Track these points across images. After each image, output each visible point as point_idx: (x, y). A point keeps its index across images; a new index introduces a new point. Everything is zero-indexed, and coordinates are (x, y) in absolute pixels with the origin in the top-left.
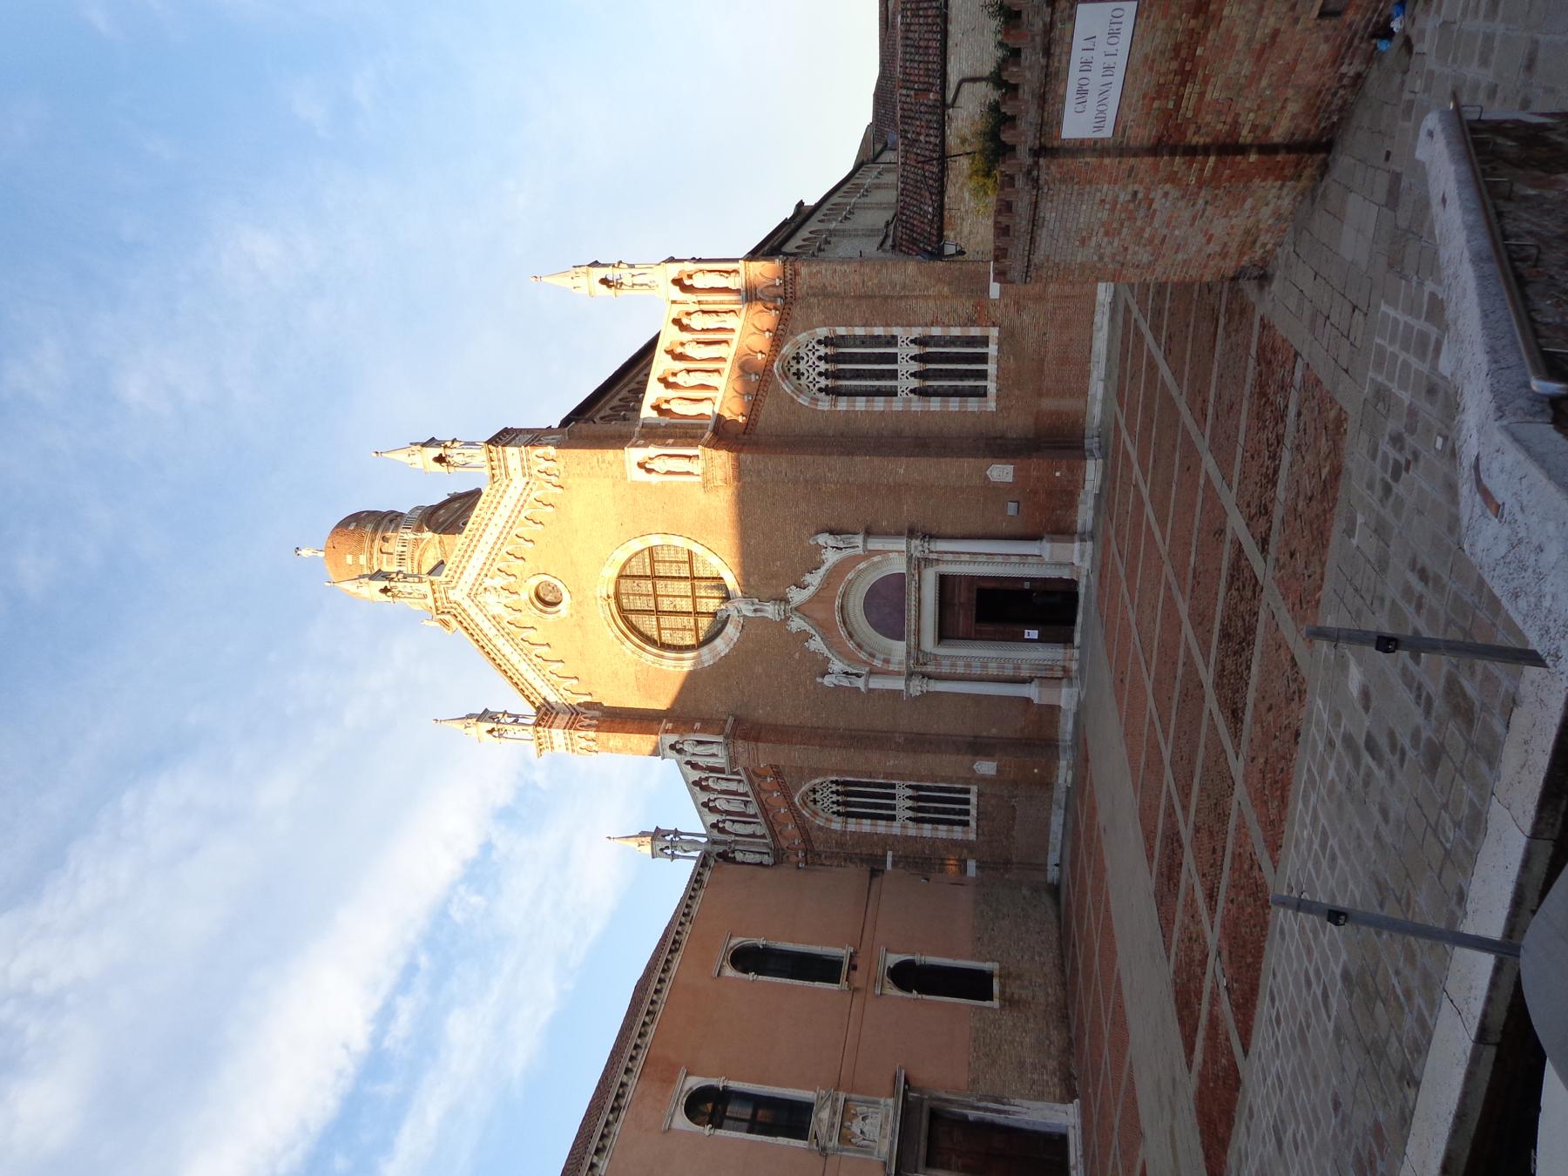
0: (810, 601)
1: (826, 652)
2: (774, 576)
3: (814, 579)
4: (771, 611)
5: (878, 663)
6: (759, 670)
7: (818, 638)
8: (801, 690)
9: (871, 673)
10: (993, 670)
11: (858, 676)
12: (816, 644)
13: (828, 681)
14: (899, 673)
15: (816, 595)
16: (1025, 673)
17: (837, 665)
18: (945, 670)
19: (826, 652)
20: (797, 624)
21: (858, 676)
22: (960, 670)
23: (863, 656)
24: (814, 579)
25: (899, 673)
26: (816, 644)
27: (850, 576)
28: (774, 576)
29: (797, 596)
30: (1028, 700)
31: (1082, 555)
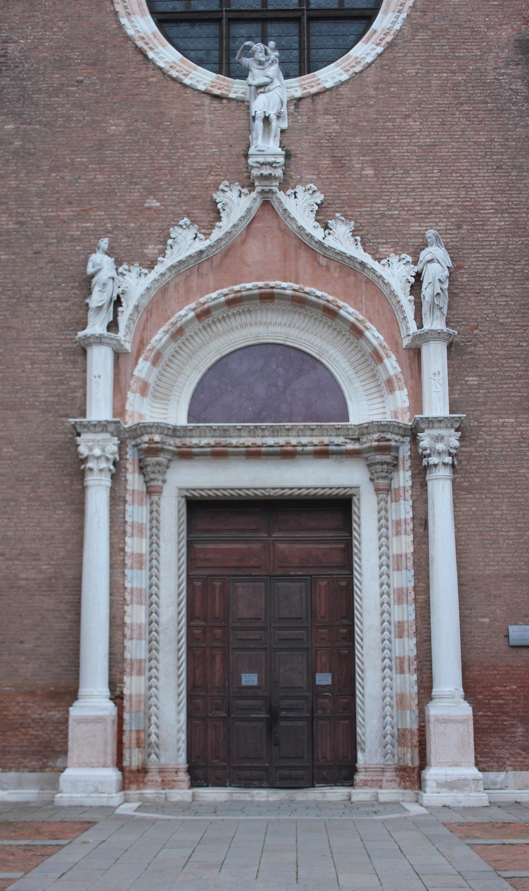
0: (285, 231)
1: (171, 258)
2: (339, 164)
3: (341, 238)
4: (266, 147)
5: (142, 368)
6: (115, 127)
7: (201, 245)
8: (67, 212)
9: (118, 356)
10: (136, 615)
11: (113, 326)
12: (186, 242)
13: (101, 262)
14: (119, 410)
15: (303, 243)
16: (133, 685)
17: (137, 284)
18: (136, 513)
19: (171, 258)
20: (236, 205)
21: (113, 326)
22: (136, 545)
23: (159, 338)
24: (341, 238)
25: (119, 410)
26: (186, 242)
27: (349, 311)
28: (339, 164)
29: (300, 207)
30: (70, 693)
31: (451, 785)
